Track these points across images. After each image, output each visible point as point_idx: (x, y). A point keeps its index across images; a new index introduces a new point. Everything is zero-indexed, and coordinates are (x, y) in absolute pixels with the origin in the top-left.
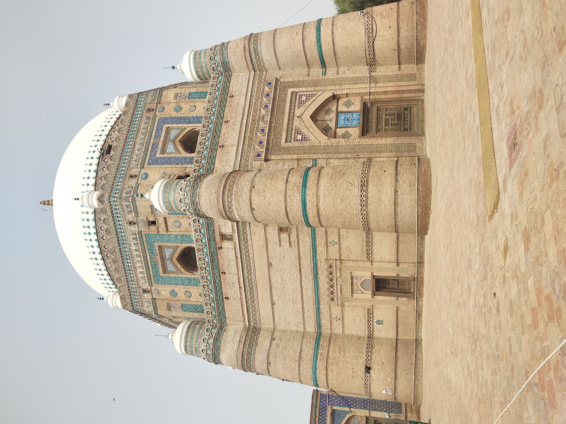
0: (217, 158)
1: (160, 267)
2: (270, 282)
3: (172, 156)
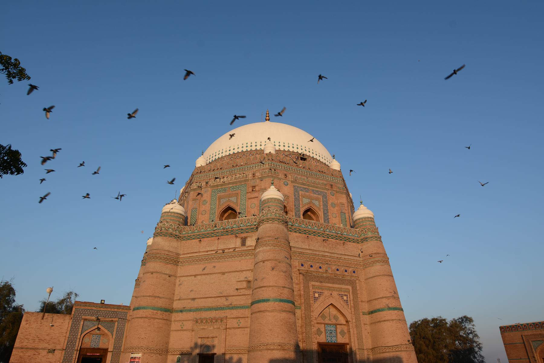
0: (300, 234)
1: (223, 194)
2: (211, 274)
3: (301, 202)
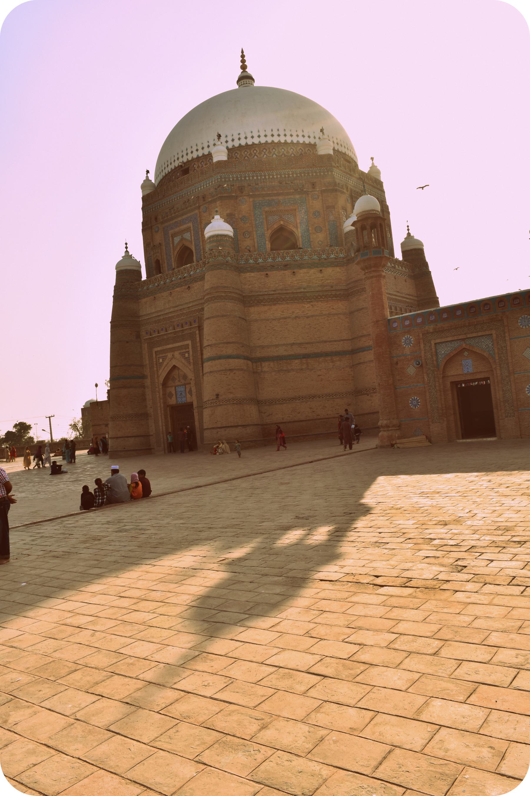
3: (171, 245)
